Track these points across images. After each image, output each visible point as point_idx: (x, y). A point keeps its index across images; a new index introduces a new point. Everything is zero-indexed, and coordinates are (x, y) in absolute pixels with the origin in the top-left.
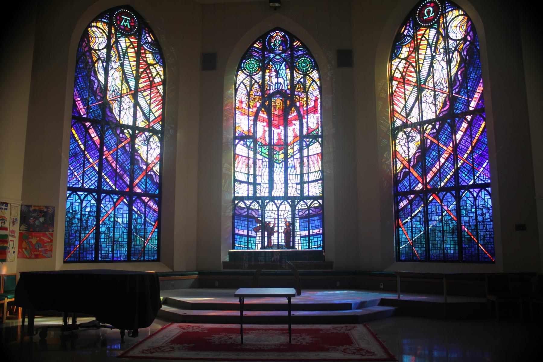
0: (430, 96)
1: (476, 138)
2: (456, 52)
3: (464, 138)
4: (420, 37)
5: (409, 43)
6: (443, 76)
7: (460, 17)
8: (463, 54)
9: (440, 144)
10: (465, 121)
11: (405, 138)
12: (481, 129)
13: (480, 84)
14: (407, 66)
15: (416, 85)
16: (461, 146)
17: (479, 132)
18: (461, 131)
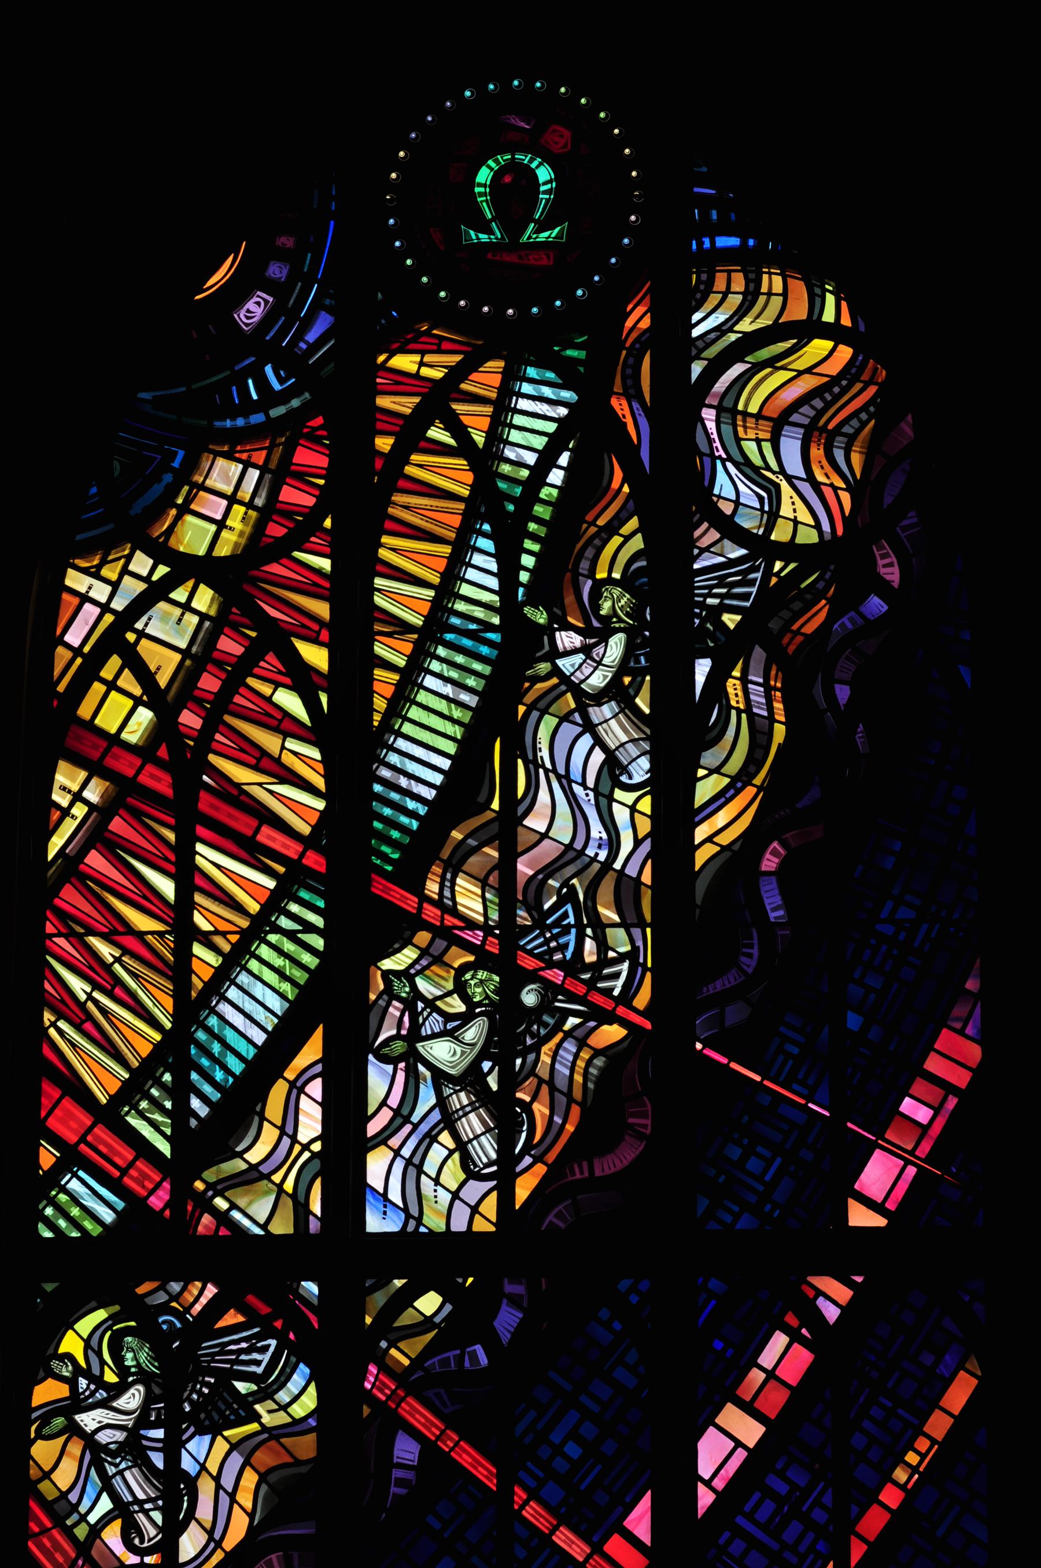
0: (456, 1005)
1: (891, 1497)
2: (759, 654)
3: (773, 1482)
4: (404, 405)
5: (272, 427)
6: (613, 843)
7: (820, 346)
8: (818, 691)
9: (520, 1494)
10: (791, 1319)
11: (144, 1377)
12: (938, 1425)
13: (960, 1010)
14: (229, 646)
15: (314, 860)
16: (738, 1546)
17: (923, 1444)
18: (749, 1409)
